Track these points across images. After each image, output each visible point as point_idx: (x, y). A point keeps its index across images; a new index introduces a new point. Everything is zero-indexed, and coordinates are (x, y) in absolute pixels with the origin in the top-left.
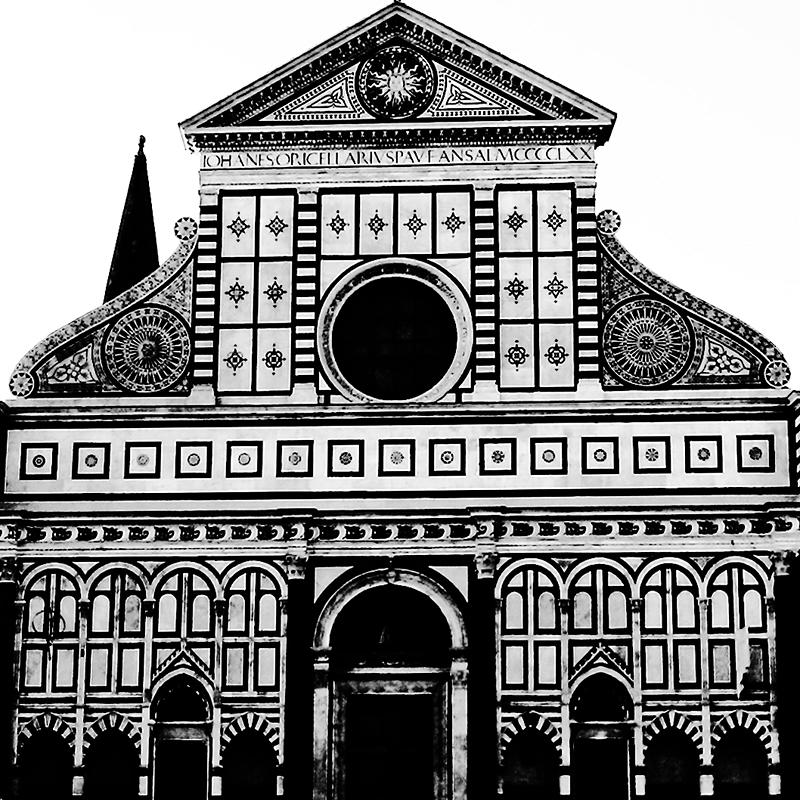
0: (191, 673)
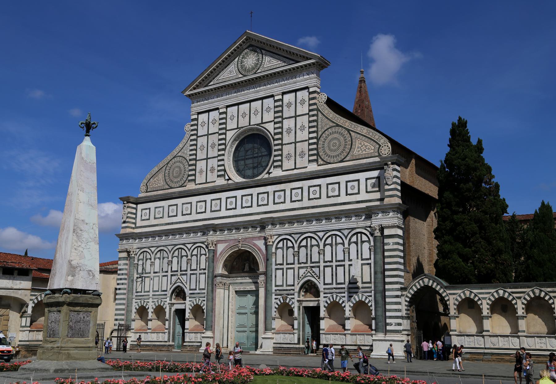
0: (181, 285)
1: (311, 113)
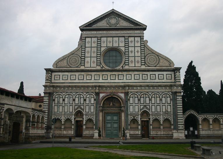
0: (80, 110)
1: (142, 47)
